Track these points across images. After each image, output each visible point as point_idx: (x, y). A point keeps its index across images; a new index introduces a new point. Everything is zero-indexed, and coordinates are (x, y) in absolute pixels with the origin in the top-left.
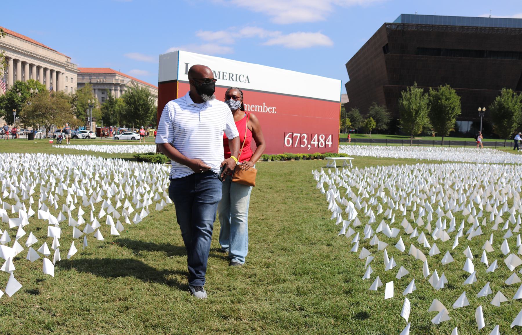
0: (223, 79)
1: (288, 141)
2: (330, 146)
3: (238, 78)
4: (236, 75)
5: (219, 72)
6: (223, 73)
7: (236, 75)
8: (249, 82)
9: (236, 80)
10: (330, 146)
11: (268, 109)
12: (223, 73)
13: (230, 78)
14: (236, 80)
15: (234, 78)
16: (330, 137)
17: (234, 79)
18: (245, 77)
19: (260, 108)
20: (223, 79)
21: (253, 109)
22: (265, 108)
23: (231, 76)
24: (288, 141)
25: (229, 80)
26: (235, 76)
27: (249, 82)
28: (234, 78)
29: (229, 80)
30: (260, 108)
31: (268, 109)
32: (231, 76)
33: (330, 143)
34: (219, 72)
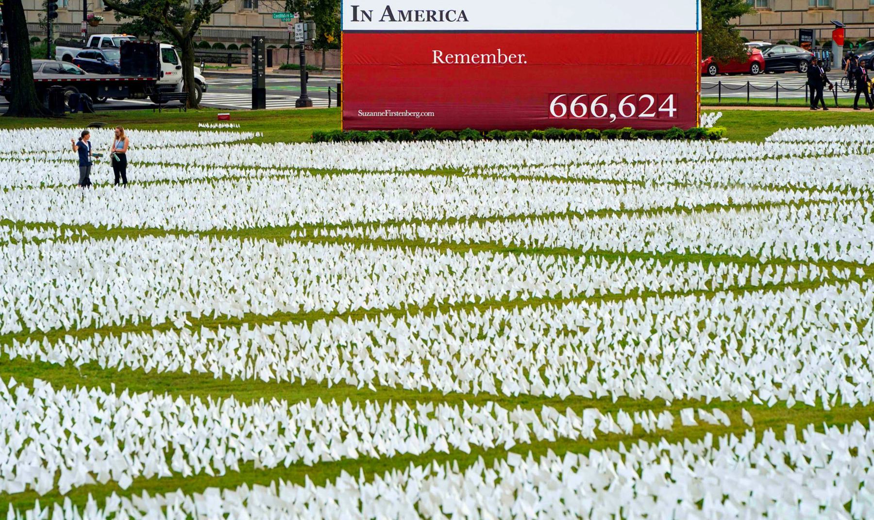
0: (417, 20)
1: (558, 110)
2: (671, 115)
3: (445, 16)
4: (441, 12)
6: (417, 12)
7: (441, 12)
8: (466, 20)
9: (441, 20)
10: (671, 115)
11: (508, 59)
12: (417, 12)
13: (431, 16)
14: (441, 20)
15: (437, 17)
16: (671, 97)
18: (459, 13)
19: (491, 58)
20: (417, 20)
21: (476, 60)
22: (503, 59)
23: (431, 13)
24: (558, 110)
25: (429, 20)
26: (438, 14)
27: (466, 20)
28: (437, 17)
29: (429, 20)
30: (491, 58)
31: (508, 59)
33: (671, 110)
34: (410, 12)
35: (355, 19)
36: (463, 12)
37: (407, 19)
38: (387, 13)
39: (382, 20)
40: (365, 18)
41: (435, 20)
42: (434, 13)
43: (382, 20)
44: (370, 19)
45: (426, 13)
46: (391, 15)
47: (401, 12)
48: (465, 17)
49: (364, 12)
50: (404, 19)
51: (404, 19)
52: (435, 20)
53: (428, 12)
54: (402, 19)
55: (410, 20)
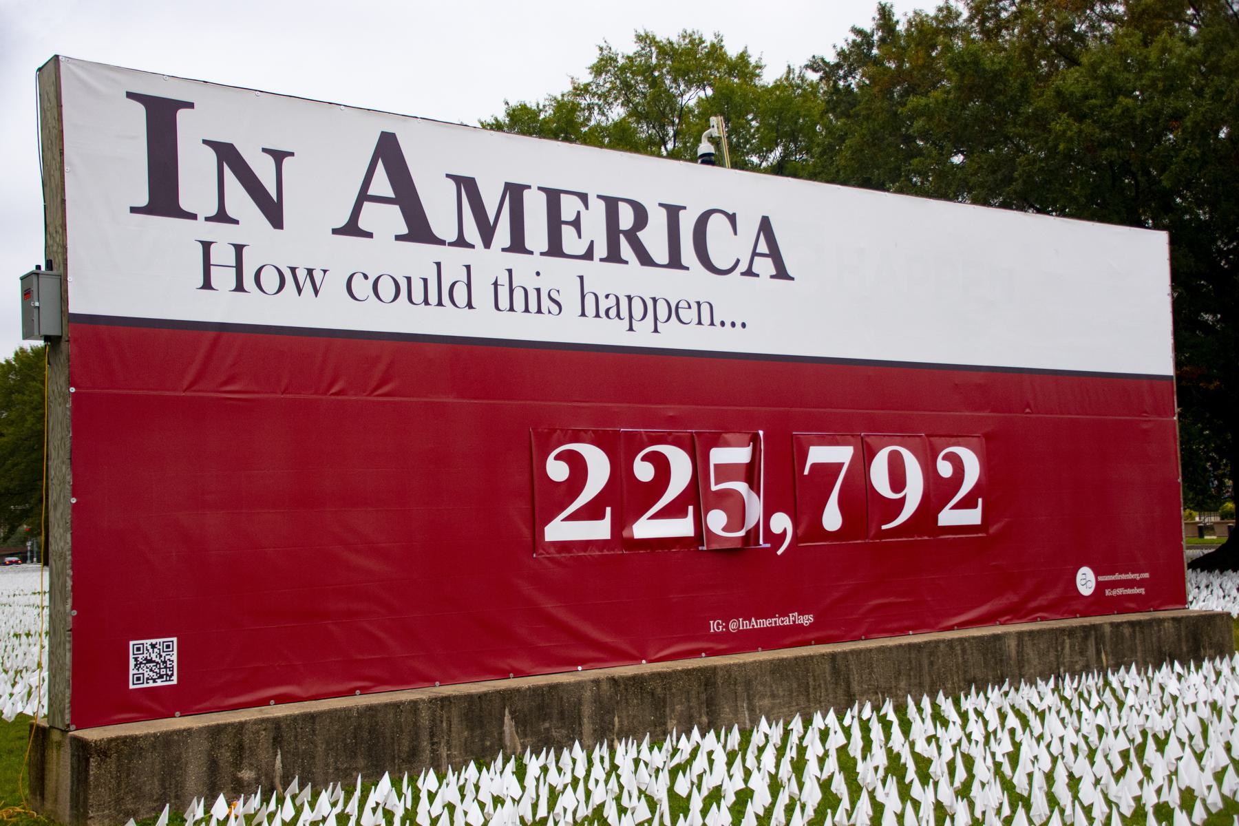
0: (555, 249)
4: (673, 212)
5: (514, 192)
7: (673, 212)
8: (781, 273)
9: (675, 262)
12: (553, 197)
15: (655, 238)
17: (660, 253)
20: (555, 249)
23: (626, 219)
27: (781, 273)
28: (655, 238)
29: (614, 256)
32: (626, 219)
35: (163, 198)
36: (765, 226)
37: (503, 235)
38: (382, 185)
39: (351, 228)
40: (238, 200)
41: (645, 259)
42: (641, 216)
43: (351, 228)
44: (273, 211)
45: (598, 210)
46: (406, 197)
47: (467, 186)
48: (775, 254)
49: (227, 155)
50: (487, 233)
51: (487, 233)
52: (645, 259)
53: (612, 205)
54: (472, 232)
55: (518, 245)
